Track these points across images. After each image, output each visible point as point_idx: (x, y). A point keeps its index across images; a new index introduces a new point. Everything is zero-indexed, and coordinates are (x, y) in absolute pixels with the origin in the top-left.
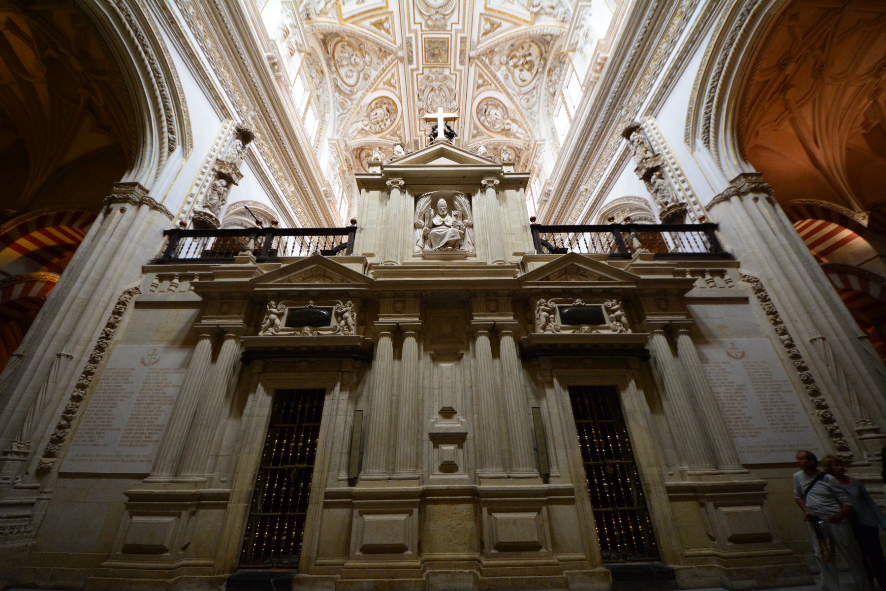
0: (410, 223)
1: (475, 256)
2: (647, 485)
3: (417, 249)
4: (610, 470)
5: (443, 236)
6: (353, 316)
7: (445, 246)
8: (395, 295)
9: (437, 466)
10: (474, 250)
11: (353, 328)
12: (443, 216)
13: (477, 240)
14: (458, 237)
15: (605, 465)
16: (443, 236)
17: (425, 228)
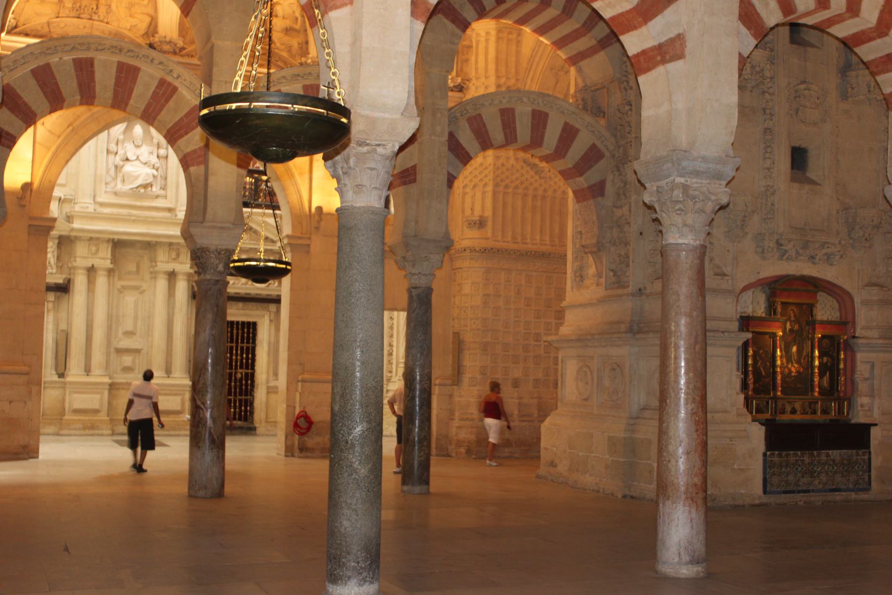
0: (102, 152)
1: (166, 197)
2: (258, 385)
3: (109, 179)
4: (239, 376)
5: (137, 177)
6: (54, 257)
7: (137, 188)
8: (91, 239)
9: (119, 369)
10: (166, 185)
11: (54, 267)
12: (138, 147)
13: (169, 179)
14: (151, 180)
15: (236, 373)
16: (137, 177)
17: (118, 158)
